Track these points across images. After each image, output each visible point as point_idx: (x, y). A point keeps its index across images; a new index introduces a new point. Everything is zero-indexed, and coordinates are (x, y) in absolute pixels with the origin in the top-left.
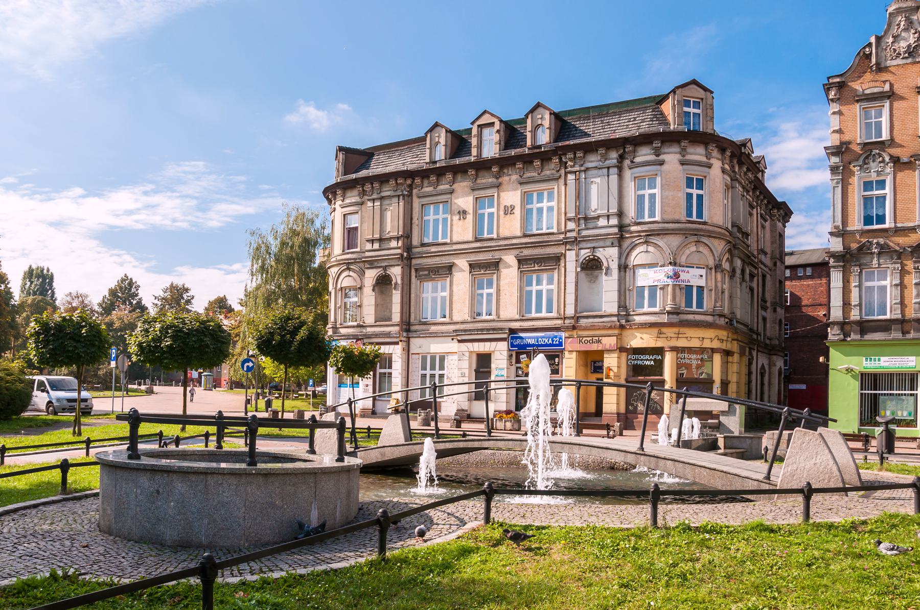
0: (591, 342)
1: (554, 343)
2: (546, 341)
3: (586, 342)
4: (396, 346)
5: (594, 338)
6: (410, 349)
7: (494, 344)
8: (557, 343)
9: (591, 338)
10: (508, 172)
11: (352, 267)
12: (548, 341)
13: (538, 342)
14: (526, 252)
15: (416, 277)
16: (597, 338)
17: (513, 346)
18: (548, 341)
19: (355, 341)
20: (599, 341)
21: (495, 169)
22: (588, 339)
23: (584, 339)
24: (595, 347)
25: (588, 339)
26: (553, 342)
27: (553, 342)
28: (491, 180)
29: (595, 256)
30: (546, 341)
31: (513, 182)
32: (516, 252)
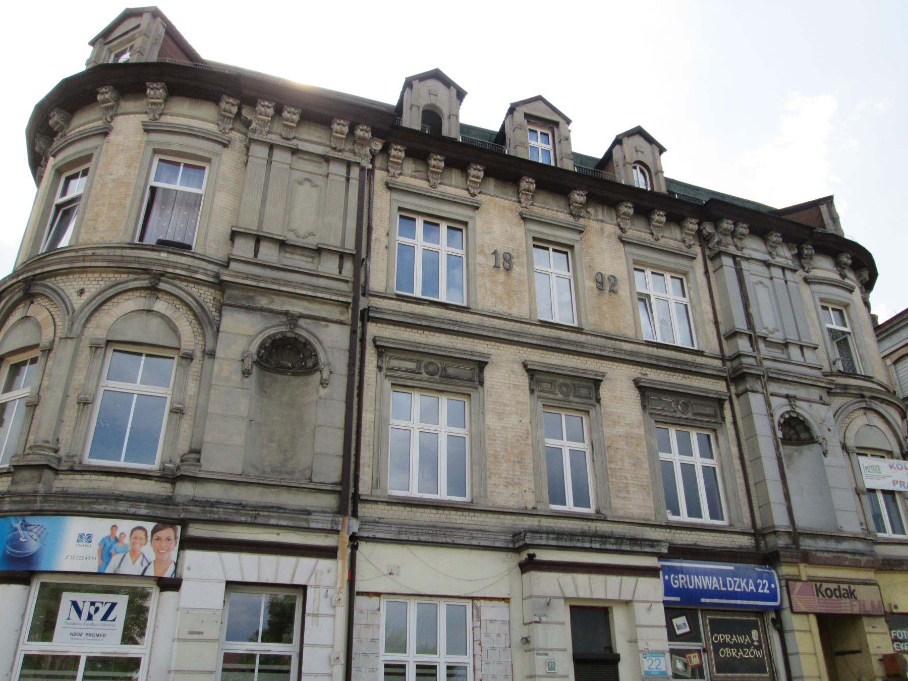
0: (846, 595)
1: (760, 591)
2: (743, 585)
3: (829, 592)
4: (324, 564)
5: (843, 586)
6: (357, 577)
7: (629, 581)
8: (767, 591)
9: (835, 586)
10: (596, 215)
11: (162, 286)
12: (747, 584)
13: (725, 585)
14: (655, 376)
15: (380, 368)
16: (846, 586)
17: (669, 590)
18: (747, 584)
19: (150, 526)
20: (851, 594)
21: (578, 197)
22: (833, 586)
23: (825, 586)
24: (846, 607)
25: (833, 586)
26: (757, 588)
27: (757, 588)
28: (563, 217)
29: (798, 413)
30: (743, 585)
31: (609, 236)
32: (635, 372)
